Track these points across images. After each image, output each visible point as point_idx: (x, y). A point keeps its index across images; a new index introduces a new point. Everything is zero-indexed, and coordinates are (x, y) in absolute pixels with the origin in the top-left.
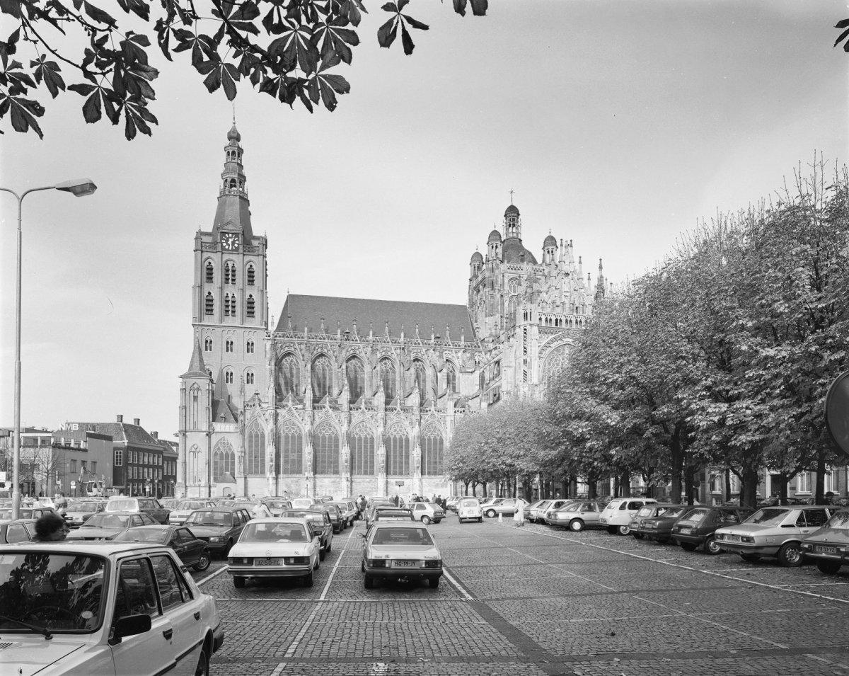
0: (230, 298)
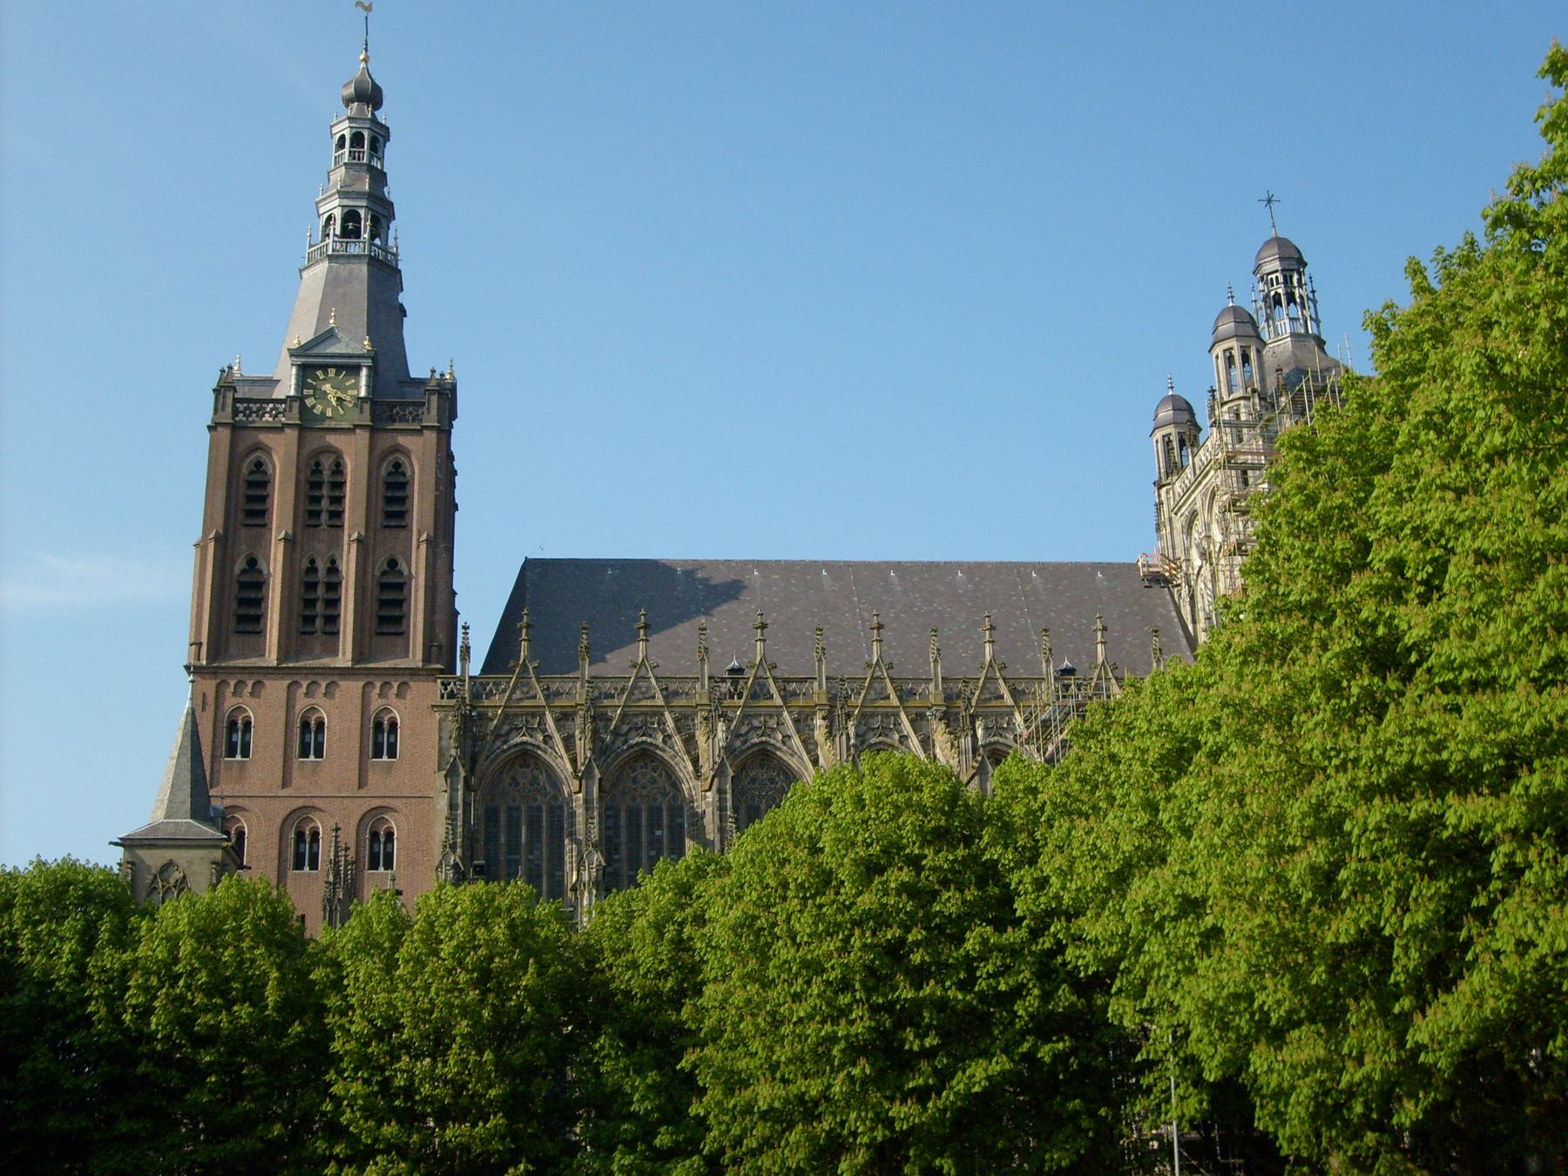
0: (322, 574)
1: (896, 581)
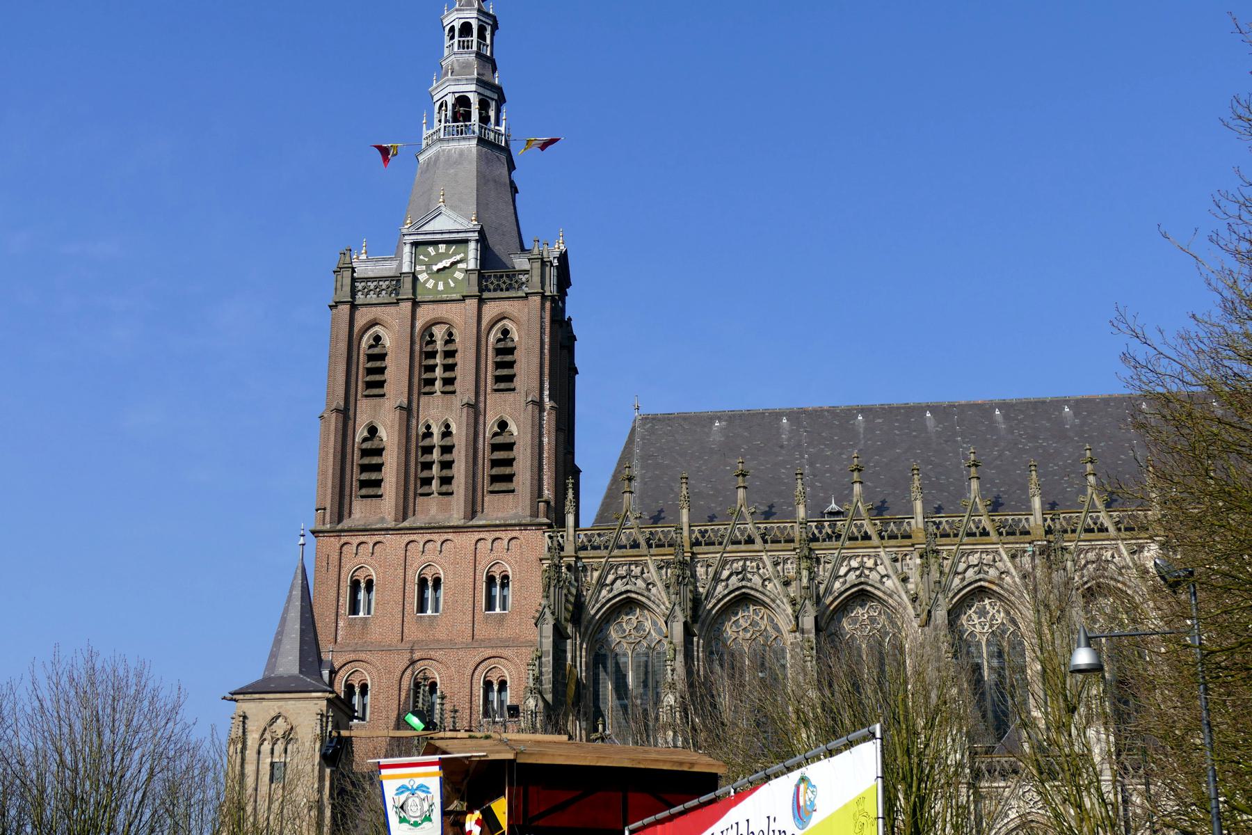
0: (436, 439)
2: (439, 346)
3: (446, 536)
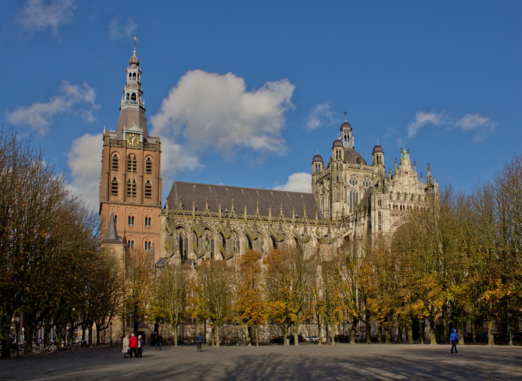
0: (131, 183)
1: (258, 193)
2: (132, 160)
3: (136, 207)
